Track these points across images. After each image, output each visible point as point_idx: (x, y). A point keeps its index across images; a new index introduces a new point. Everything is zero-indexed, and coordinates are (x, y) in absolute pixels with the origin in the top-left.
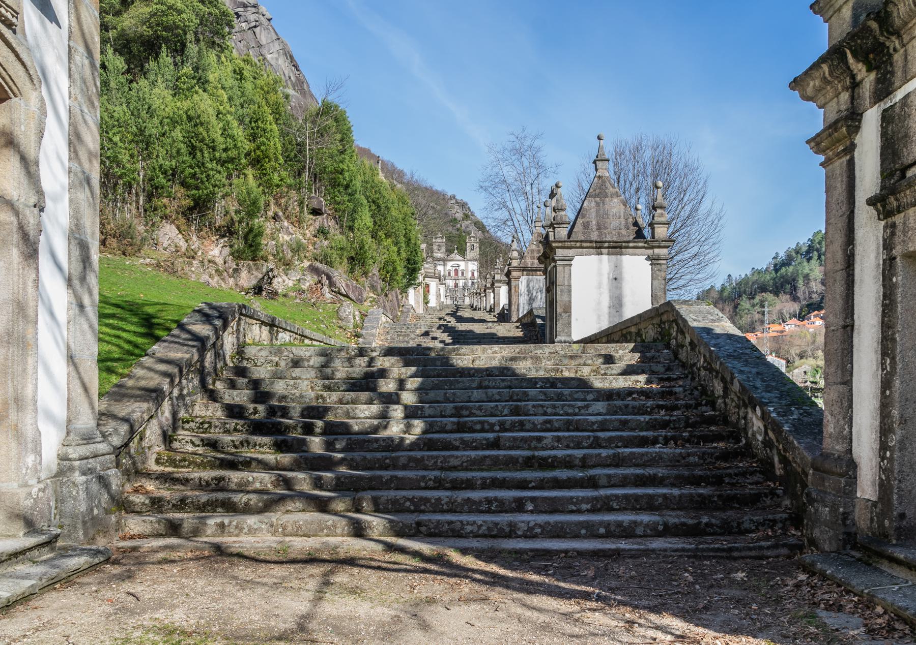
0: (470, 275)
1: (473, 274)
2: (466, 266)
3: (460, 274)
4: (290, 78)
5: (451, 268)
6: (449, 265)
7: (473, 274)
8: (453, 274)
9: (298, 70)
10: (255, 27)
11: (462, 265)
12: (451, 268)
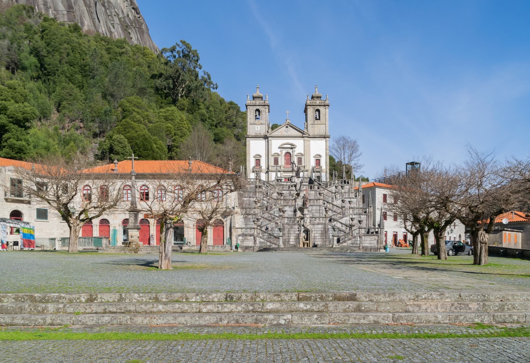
0: (313, 163)
1: (318, 162)
2: (307, 148)
4: (128, 16)
5: (278, 151)
6: (275, 144)
7: (318, 162)
8: (282, 161)
9: (138, 14)
11: (299, 144)
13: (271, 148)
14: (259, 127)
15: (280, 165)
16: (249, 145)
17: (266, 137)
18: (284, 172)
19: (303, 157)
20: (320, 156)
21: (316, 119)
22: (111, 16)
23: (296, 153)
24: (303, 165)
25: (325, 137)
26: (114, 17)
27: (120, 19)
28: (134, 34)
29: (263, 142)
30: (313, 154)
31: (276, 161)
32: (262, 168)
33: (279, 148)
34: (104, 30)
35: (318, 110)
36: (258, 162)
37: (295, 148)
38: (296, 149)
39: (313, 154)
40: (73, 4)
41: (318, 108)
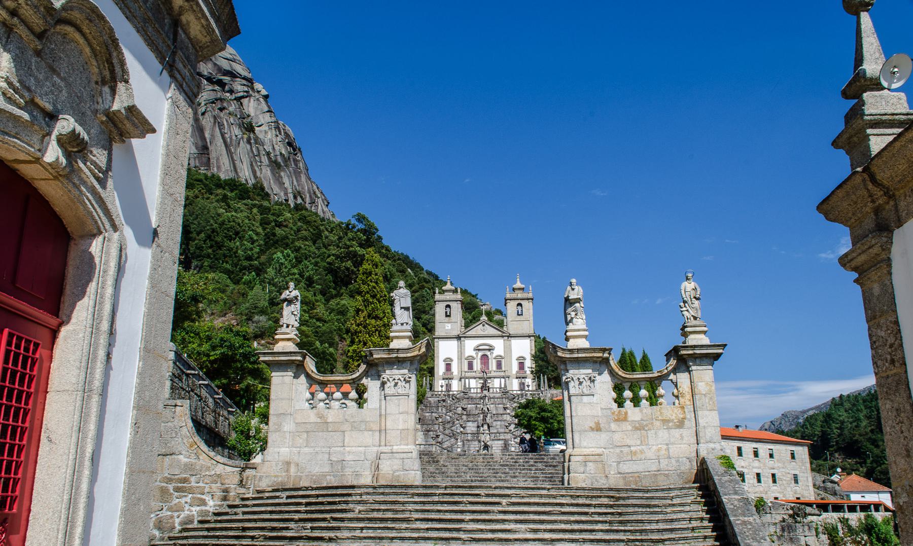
0: (515, 368)
1: (521, 366)
2: (508, 349)
3: (493, 365)
5: (473, 354)
6: (470, 346)
8: (477, 365)
11: (499, 345)
12: (473, 354)
13: (464, 349)
14: (449, 325)
15: (475, 370)
16: (438, 347)
17: (459, 338)
18: (479, 378)
19: (503, 361)
20: (524, 359)
21: (519, 315)
22: (259, 155)
23: (494, 355)
24: (503, 369)
25: (529, 336)
26: (262, 157)
27: (269, 158)
28: (288, 176)
29: (454, 343)
30: (515, 355)
31: (470, 366)
32: (454, 374)
33: (475, 350)
34: (247, 174)
35: (520, 305)
36: (448, 367)
37: (492, 349)
38: (494, 352)
39: (515, 355)
40: (209, 143)
41: (521, 302)
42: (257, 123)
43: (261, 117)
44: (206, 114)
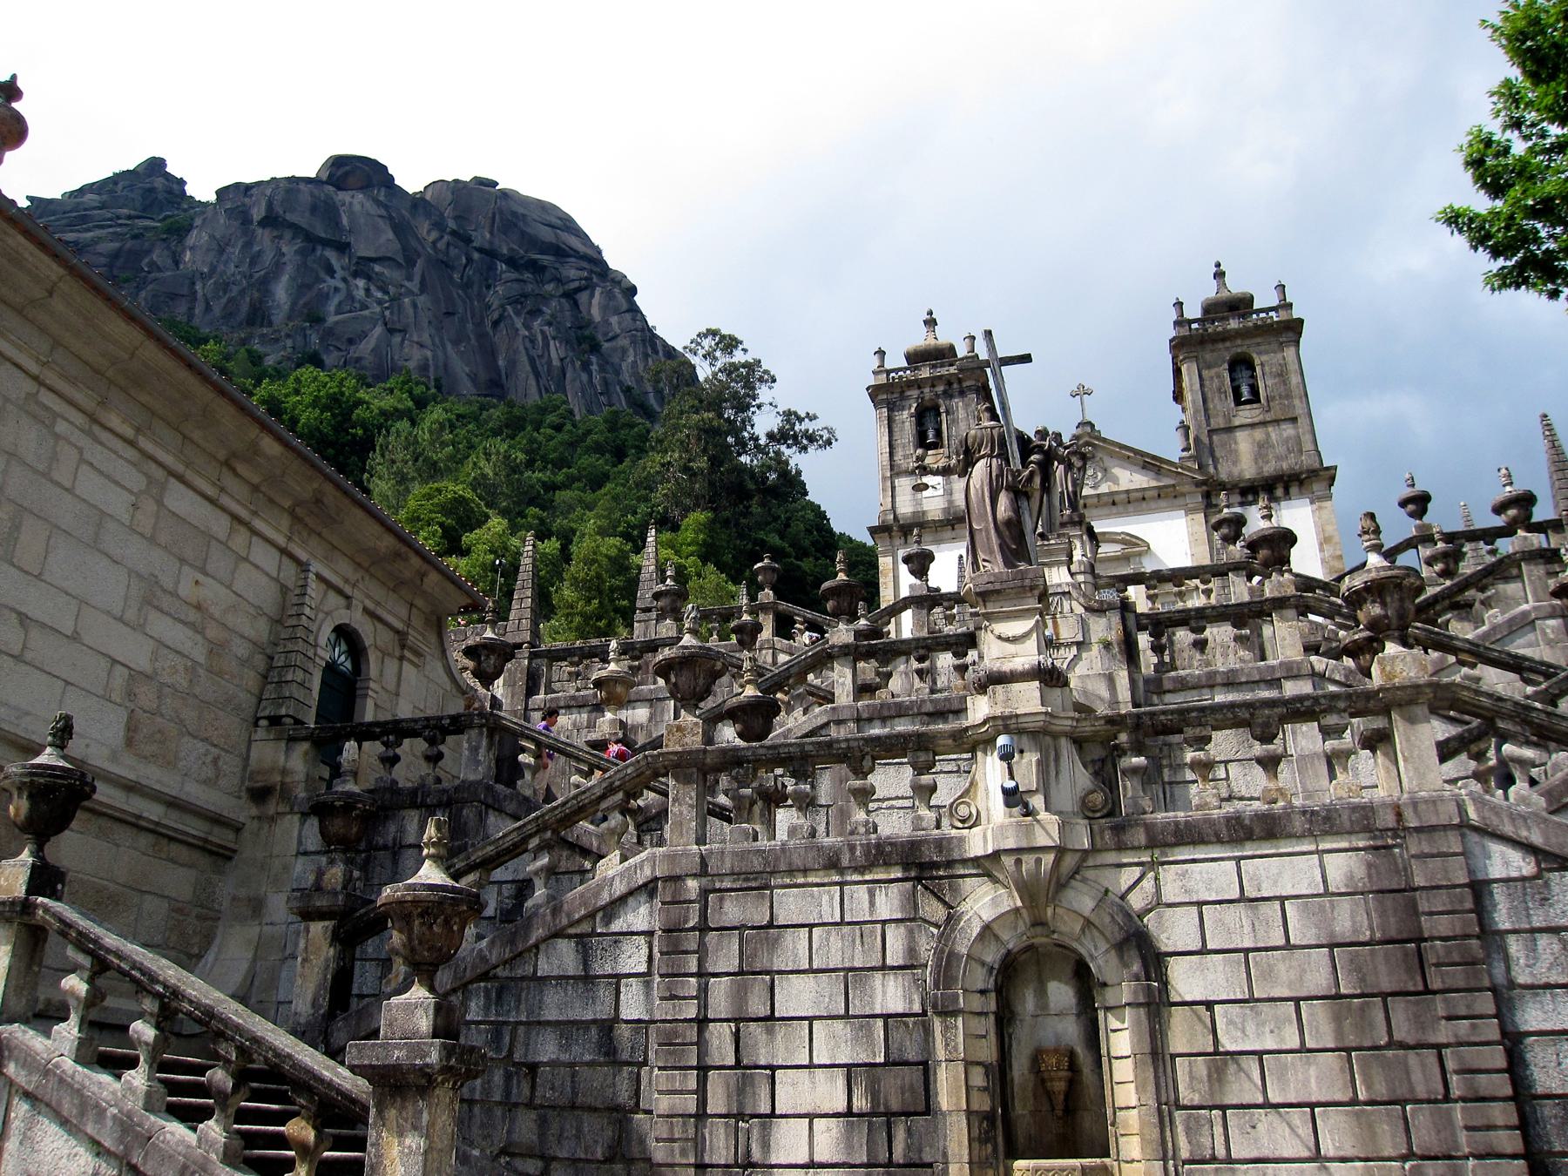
10: (579, 290)
22: (606, 392)
37: (1140, 554)
40: (504, 377)
42: (605, 334)
43: (614, 320)
44: (502, 325)
